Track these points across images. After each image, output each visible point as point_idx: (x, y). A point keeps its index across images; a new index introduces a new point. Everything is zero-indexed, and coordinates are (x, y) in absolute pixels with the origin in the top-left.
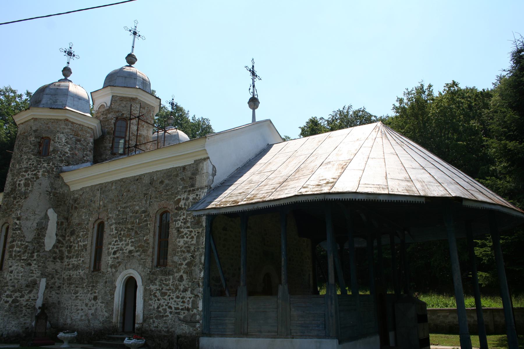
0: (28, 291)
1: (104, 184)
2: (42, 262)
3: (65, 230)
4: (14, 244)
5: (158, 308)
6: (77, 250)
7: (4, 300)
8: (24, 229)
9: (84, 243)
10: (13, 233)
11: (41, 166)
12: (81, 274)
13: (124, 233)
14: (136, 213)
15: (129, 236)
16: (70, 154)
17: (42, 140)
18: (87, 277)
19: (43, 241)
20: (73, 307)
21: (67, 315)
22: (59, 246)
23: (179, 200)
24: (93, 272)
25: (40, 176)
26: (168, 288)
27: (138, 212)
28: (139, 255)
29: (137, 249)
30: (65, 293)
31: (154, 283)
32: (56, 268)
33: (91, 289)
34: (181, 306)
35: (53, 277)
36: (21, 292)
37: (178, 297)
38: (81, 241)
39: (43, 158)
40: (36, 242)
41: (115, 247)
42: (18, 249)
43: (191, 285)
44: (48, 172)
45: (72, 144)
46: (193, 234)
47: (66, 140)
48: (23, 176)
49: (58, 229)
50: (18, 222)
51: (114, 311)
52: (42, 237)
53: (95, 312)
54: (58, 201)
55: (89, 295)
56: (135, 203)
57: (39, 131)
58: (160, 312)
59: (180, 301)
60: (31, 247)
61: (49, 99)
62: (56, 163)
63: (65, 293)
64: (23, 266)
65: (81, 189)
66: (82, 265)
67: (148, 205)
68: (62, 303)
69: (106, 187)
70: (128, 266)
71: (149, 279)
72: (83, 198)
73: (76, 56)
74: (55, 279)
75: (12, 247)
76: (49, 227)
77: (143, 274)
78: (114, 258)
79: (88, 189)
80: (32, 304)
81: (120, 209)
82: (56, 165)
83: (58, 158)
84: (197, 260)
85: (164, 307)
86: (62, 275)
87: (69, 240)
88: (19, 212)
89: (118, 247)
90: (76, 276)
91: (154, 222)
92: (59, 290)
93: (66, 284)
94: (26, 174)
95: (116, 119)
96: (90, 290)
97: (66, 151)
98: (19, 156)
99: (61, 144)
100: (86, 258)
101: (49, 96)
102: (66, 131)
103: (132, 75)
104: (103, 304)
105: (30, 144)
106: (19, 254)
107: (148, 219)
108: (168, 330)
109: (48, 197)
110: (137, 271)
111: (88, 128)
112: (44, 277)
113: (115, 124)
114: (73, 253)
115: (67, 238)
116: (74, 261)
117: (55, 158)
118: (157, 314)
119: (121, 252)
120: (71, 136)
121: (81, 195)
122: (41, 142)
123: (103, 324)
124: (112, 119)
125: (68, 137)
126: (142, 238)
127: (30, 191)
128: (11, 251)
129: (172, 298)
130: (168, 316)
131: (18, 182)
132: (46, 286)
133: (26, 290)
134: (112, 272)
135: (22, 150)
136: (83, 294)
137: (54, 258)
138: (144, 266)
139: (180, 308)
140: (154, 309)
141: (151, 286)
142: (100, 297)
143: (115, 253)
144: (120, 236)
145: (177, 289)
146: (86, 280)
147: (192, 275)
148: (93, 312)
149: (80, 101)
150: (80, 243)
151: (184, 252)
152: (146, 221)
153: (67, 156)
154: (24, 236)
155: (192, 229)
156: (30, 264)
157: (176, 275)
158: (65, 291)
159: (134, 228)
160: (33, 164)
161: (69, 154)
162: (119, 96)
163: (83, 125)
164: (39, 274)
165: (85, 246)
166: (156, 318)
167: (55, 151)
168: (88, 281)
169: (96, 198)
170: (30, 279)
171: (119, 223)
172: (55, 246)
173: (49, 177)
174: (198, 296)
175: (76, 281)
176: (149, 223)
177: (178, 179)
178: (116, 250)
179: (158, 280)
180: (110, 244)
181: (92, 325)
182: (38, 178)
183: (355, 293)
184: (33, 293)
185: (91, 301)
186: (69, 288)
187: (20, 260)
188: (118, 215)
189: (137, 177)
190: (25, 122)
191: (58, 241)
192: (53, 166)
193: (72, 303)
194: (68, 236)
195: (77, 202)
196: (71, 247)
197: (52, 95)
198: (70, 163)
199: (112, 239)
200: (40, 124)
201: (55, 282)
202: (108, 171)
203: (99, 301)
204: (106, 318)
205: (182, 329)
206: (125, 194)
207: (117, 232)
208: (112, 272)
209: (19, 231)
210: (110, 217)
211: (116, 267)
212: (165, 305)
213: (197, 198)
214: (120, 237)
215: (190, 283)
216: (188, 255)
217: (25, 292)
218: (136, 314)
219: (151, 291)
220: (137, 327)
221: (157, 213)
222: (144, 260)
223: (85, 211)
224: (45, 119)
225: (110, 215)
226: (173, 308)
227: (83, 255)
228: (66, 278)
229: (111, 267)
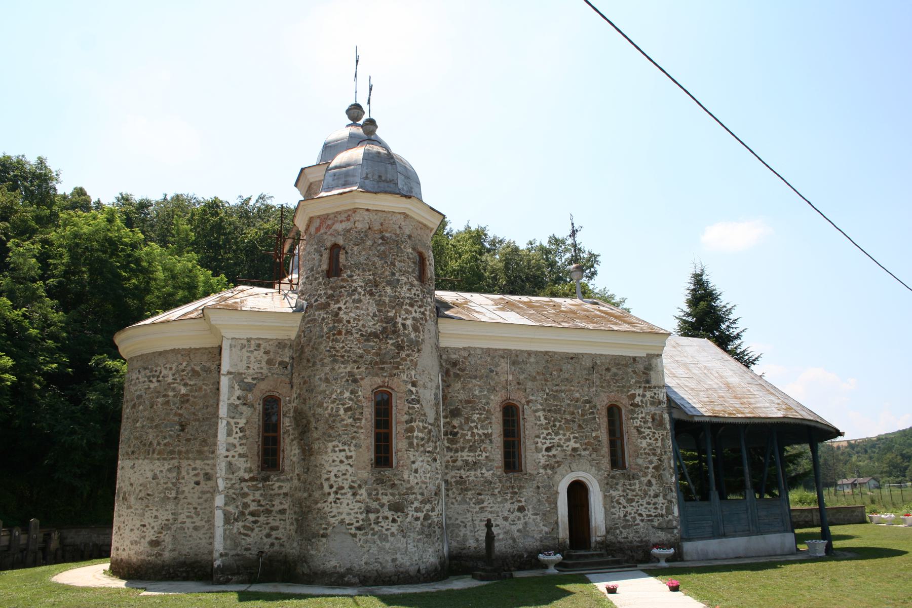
4: (413, 426)
5: (625, 516)
6: (469, 441)
7: (413, 515)
8: (424, 403)
9: (486, 432)
10: (409, 408)
12: (485, 475)
13: (560, 425)
14: (577, 402)
15: (568, 429)
21: (465, 535)
23: (634, 396)
26: (634, 493)
28: (588, 455)
29: (584, 447)
31: (615, 488)
33: (511, 497)
34: (654, 512)
36: (431, 503)
37: (649, 503)
38: (477, 428)
41: (548, 442)
42: (420, 435)
43: (663, 490)
46: (657, 436)
48: (408, 312)
50: (413, 389)
51: (560, 524)
53: (524, 528)
55: (508, 505)
56: (572, 388)
58: (628, 521)
59: (651, 508)
63: (452, 503)
64: (428, 461)
65: (464, 349)
69: (517, 356)
70: (574, 466)
71: (607, 484)
75: (411, 430)
78: (549, 456)
79: (479, 352)
84: (666, 464)
85: (632, 515)
88: (413, 373)
90: (475, 479)
96: (508, 498)
98: (387, 273)
104: (538, 517)
106: (422, 443)
107: (595, 411)
108: (642, 540)
116: (466, 455)
118: (624, 523)
119: (559, 448)
121: (464, 358)
123: (541, 541)
128: (409, 436)
129: (642, 505)
130: (639, 524)
131: (399, 320)
135: (393, 264)
138: (599, 469)
139: (653, 514)
140: (619, 518)
141: (611, 492)
142: (530, 507)
145: (646, 494)
147: (662, 479)
150: (475, 431)
151: (649, 454)
152: (592, 413)
154: (425, 415)
155: (654, 431)
157: (643, 479)
166: (624, 527)
168: (503, 486)
171: (549, 411)
174: (671, 502)
177: (630, 370)
178: (550, 445)
179: (620, 485)
180: (538, 437)
183: (761, 496)
185: (512, 513)
186: (462, 495)
187: (425, 452)
188: (546, 400)
189: (572, 356)
195: (458, 367)
202: (532, 337)
203: (529, 513)
205: (659, 537)
208: (546, 474)
209: (418, 406)
210: (532, 400)
212: (633, 513)
213: (656, 397)
215: (661, 489)
216: (655, 459)
219: (612, 497)
223: (478, 383)
225: (531, 397)
226: (645, 516)
227: (485, 448)
229: (545, 467)
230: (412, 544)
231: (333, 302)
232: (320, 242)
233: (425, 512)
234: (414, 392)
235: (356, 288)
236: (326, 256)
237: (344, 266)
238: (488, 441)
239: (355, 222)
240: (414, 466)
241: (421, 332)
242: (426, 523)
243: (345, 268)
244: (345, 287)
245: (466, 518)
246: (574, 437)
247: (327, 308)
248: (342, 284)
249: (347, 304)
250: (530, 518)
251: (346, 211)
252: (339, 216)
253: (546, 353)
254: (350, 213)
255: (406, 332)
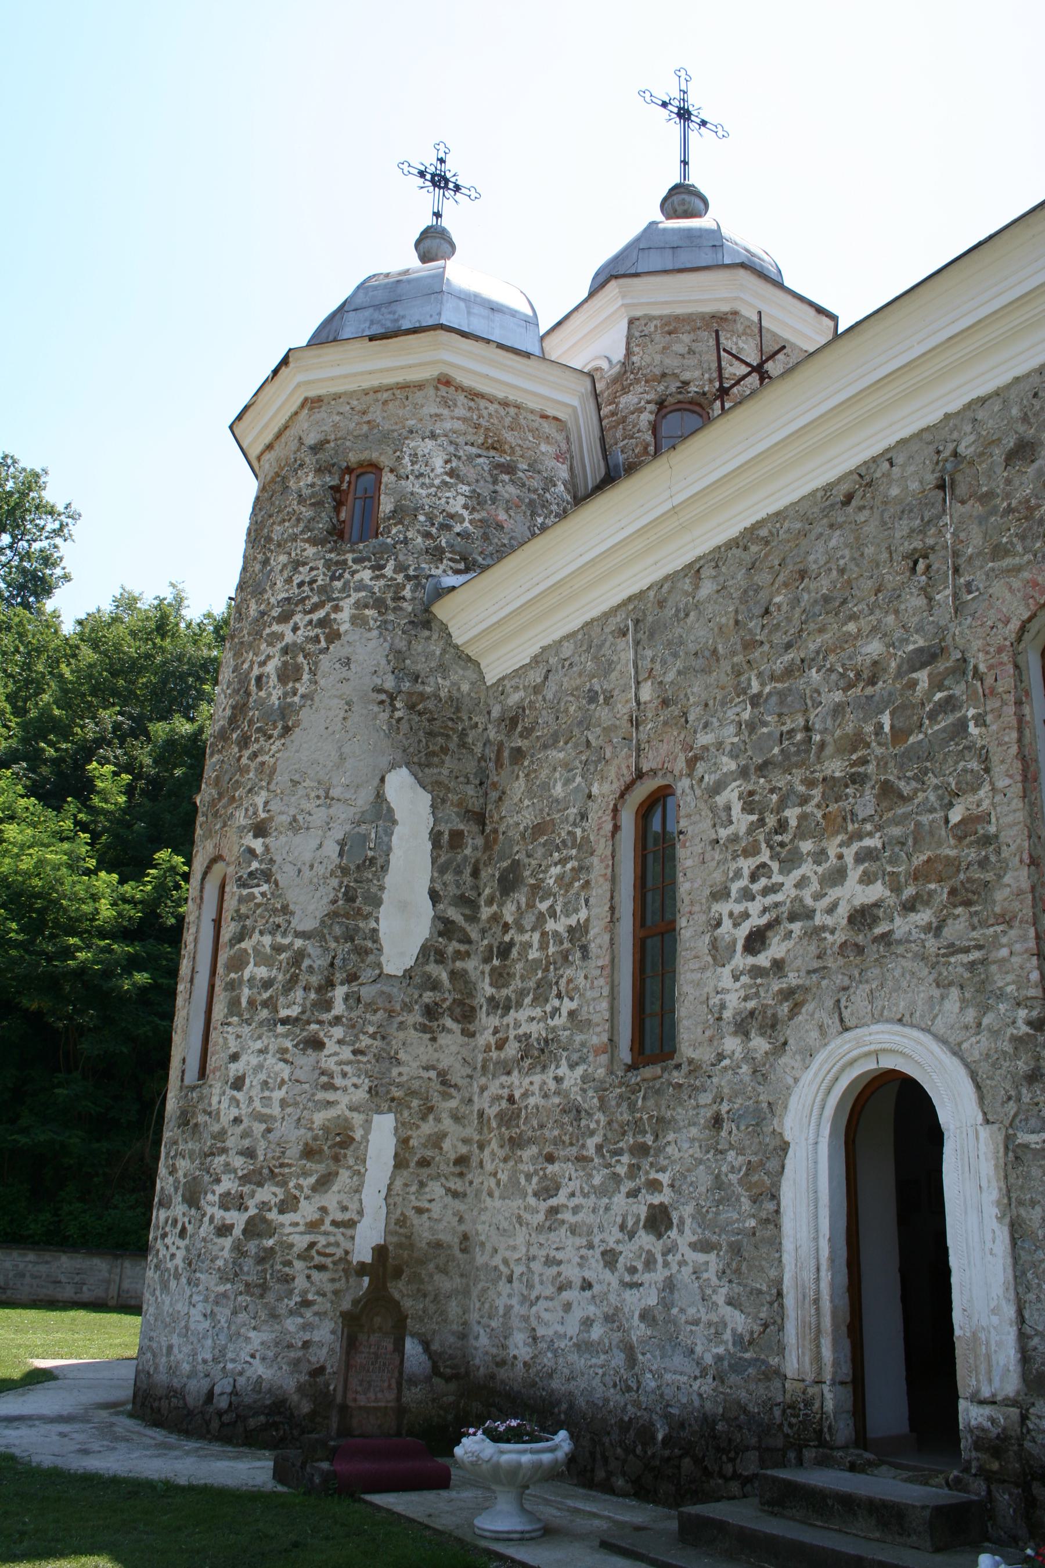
0: (312, 1180)
1: (652, 593)
2: (371, 1030)
3: (475, 873)
4: (245, 950)
8: (284, 876)
9: (572, 921)
10: (242, 899)
11: (346, 584)
12: (566, 1084)
13: (803, 817)
14: (872, 681)
15: (835, 824)
16: (471, 522)
17: (347, 477)
18: (601, 1099)
19: (373, 925)
20: (537, 1266)
21: (509, 1308)
22: (450, 950)
24: (632, 1067)
25: (343, 628)
27: (885, 670)
28: (927, 928)
29: (909, 891)
30: (490, 1194)
32: (443, 1065)
33: (631, 1166)
35: (427, 1111)
36: (284, 1184)
38: (553, 913)
39: (353, 551)
40: (337, 930)
41: (754, 907)
42: (262, 972)
44: (379, 604)
45: (477, 481)
47: (446, 462)
49: (440, 868)
50: (258, 845)
51: (790, 1301)
52: (367, 909)
53: (666, 1304)
54: (431, 734)
55: (619, 1200)
56: (851, 627)
57: (332, 444)
60: (317, 958)
61: (367, 325)
62: (410, 561)
63: (490, 1194)
64: (284, 1051)
65: (536, 660)
66: (570, 1039)
67: (943, 614)
68: (482, 1244)
69: (661, 604)
70: (858, 1002)
72: (550, 696)
73: (463, 190)
74: (438, 1120)
75: (238, 963)
76: (396, 859)
77: (977, 1046)
78: (756, 972)
79: (567, 650)
80: (337, 1244)
81: (763, 684)
82: (411, 573)
83: (420, 540)
86: (470, 1100)
87: (495, 918)
88: (260, 801)
89: (776, 905)
90: (541, 1102)
91: (1011, 698)
92: (461, 1175)
93: (494, 1145)
94: (286, 629)
95: (659, 410)
96: (622, 1170)
97: (452, 511)
99: (427, 481)
100: (589, 994)
101: (367, 313)
102: (448, 425)
103: (700, 237)
104: (712, 1257)
105: (299, 503)
106: (266, 995)
107: (958, 690)
109: (385, 716)
110: (927, 1030)
111: (544, 417)
112: (385, 1106)
113: (655, 428)
114: (517, 983)
115: (486, 912)
117: (406, 541)
119: (797, 927)
120: (474, 450)
121: (537, 689)
122: (345, 486)
123: (720, 1378)
124: (640, 410)
125: (456, 449)
126: (939, 815)
127: (303, 696)
128: (233, 981)
132: (396, 1155)
133: (305, 1174)
134: (748, 1057)
136: (586, 1195)
137: (431, 1012)
142: (688, 1210)
143: (756, 941)
144: (779, 838)
146: (599, 1116)
148: (652, 1301)
149: (498, 317)
150: (550, 925)
152: (949, 704)
153: (458, 529)
154: (285, 910)
156: (316, 1044)
158: (492, 1182)
159: (871, 768)
160: (313, 581)
161: (466, 524)
162: (661, 317)
163: (518, 407)
164: (361, 1095)
165: (575, 934)
167: (402, 513)
168: (609, 1123)
169: (614, 675)
170: (320, 1118)
171: (762, 769)
172: (428, 952)
173: (384, 626)
175: (542, 1126)
176: (971, 712)
180: (721, 894)
181: (650, 1382)
182: (334, 636)
184: (335, 1188)
185: (632, 1235)
186: (511, 1163)
188: (752, 727)
189: (845, 488)
190: (278, 436)
191: (445, 928)
192: (400, 578)
193: (529, 1244)
194: (490, 902)
195: (519, 729)
196: (505, 951)
197: (377, 307)
198: (475, 562)
199: (733, 866)
200: (337, 418)
201: (443, 1136)
202: (667, 506)
203: (683, 1238)
204: (738, 1340)
206: (777, 599)
207: (754, 818)
208: (749, 1058)
209: (265, 888)
210: (705, 748)
211: (773, 1027)
214: (782, 845)
217: (301, 1181)
218: (957, 1332)
220: (980, 1428)
221: (1019, 640)
222: (975, 955)
223: (561, 755)
224: (351, 394)
225: (704, 739)
227: (570, 981)
228: (492, 1112)
229: (742, 1027)
230: (200, 1307)
233: (252, 1211)
234: (259, 850)
238: (578, 955)
240: (235, 1069)
241: (306, 677)
242: (252, 1247)
245: (514, 1248)
246: (859, 859)
250: (682, 1263)
253: (750, 533)
255: (262, 694)
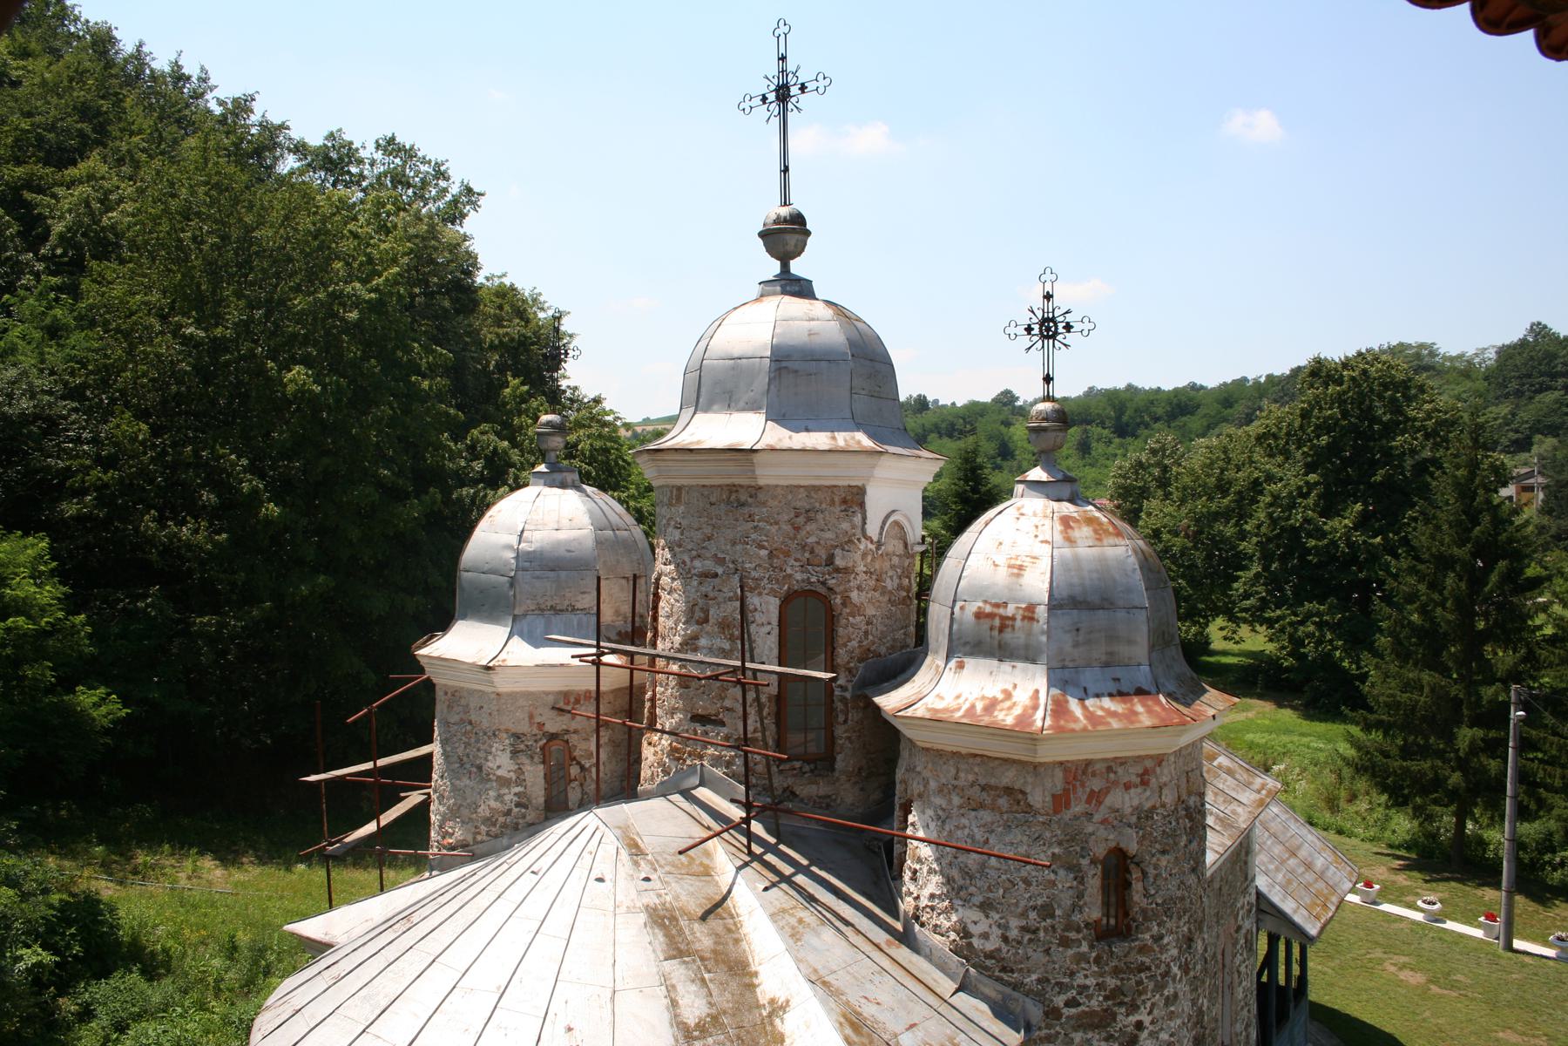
231: (1123, 1010)
232: (1074, 838)
235: (1168, 965)
236: (1094, 883)
237: (1144, 911)
239: (1161, 788)
243: (1146, 918)
244: (1149, 969)
247: (1109, 1025)
248: (1141, 958)
249: (1156, 1012)
251: (1139, 757)
252: (1120, 770)
254: (1149, 764)
